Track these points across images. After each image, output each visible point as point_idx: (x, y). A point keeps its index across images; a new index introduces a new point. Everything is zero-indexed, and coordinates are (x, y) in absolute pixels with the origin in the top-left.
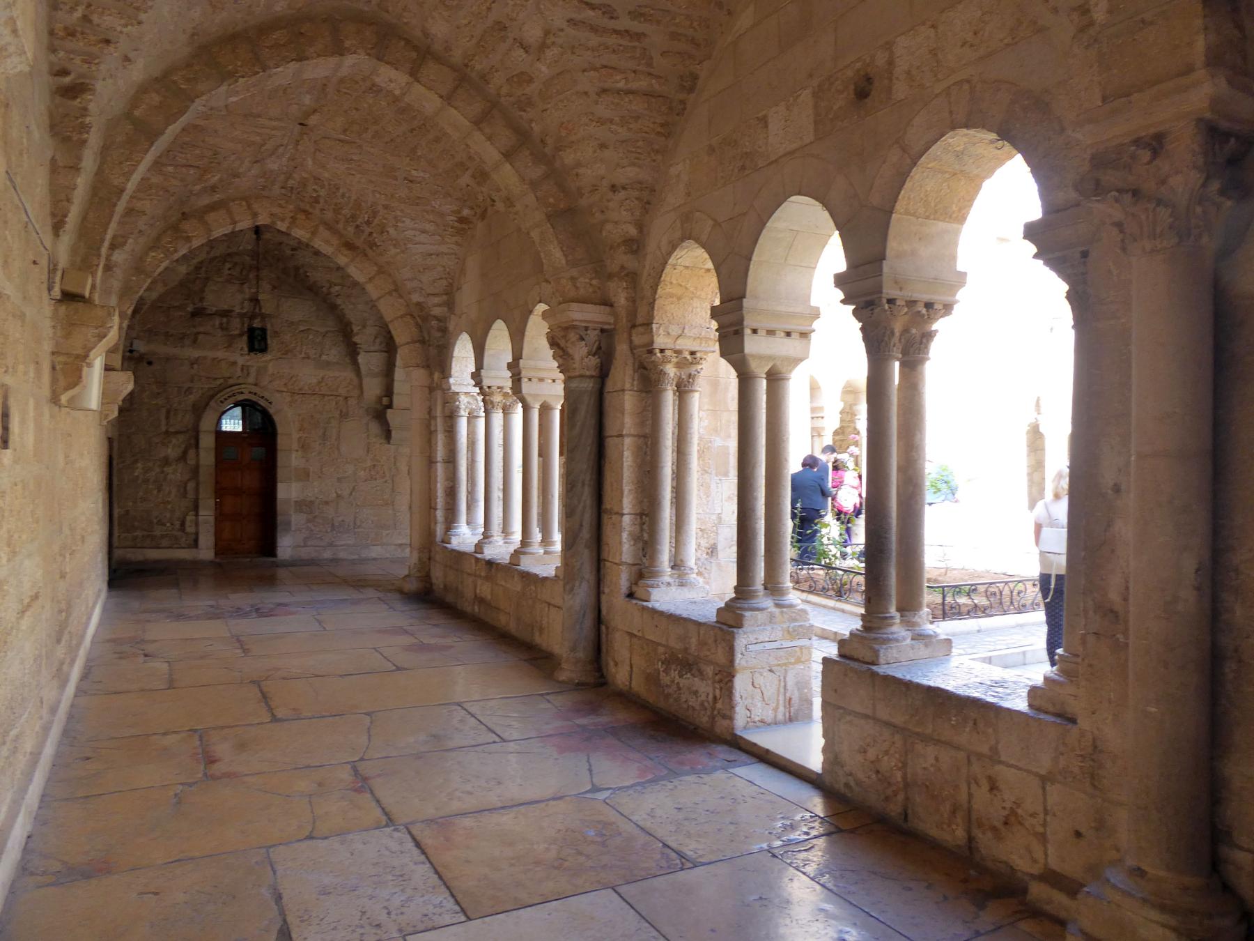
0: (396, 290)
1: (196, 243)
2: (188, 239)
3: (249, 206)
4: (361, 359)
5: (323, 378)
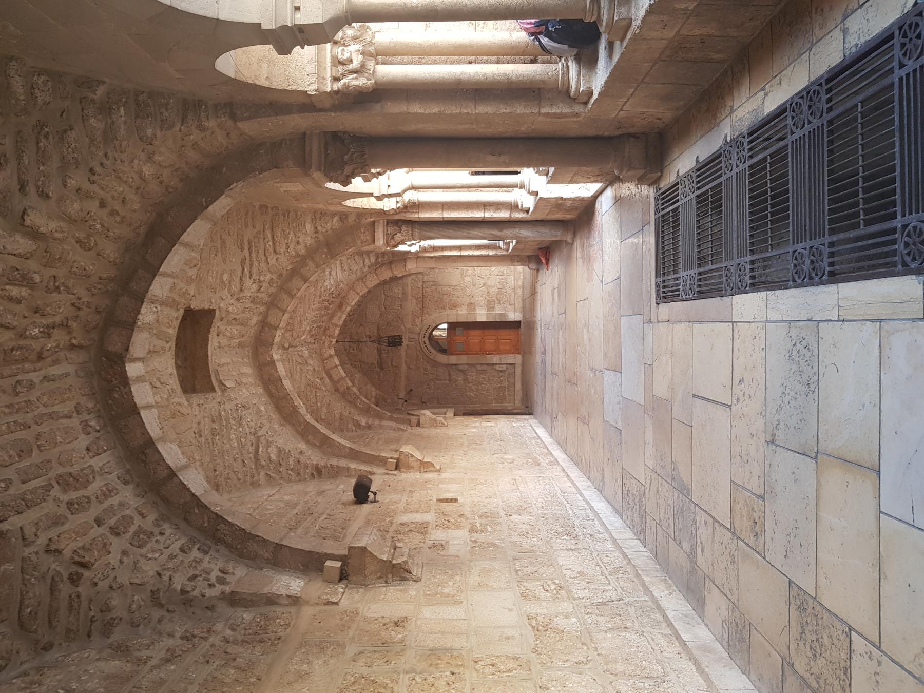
2: (348, 388)
3: (327, 359)
5: (412, 296)
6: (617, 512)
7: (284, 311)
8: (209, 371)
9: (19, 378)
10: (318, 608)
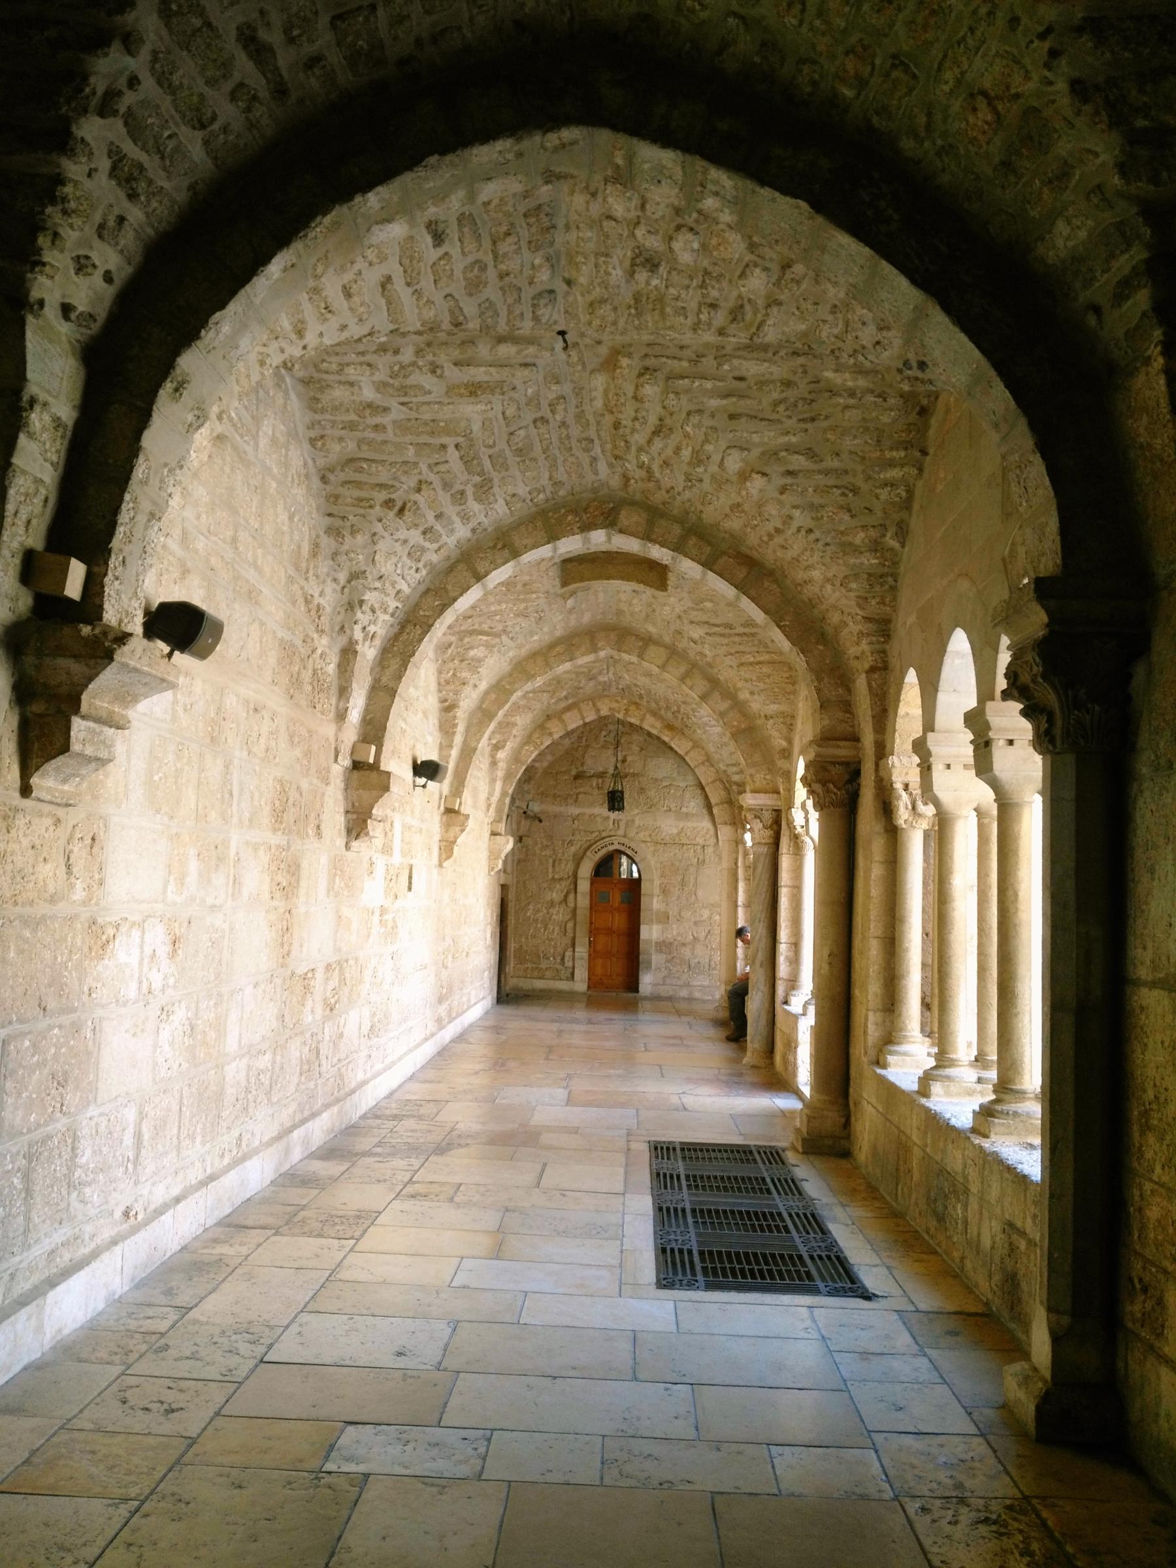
0: (708, 760)
1: (556, 736)
2: (551, 734)
4: (715, 811)
6: (391, 1094)
7: (663, 667)
8: (589, 580)
9: (597, 441)
10: (332, 740)
